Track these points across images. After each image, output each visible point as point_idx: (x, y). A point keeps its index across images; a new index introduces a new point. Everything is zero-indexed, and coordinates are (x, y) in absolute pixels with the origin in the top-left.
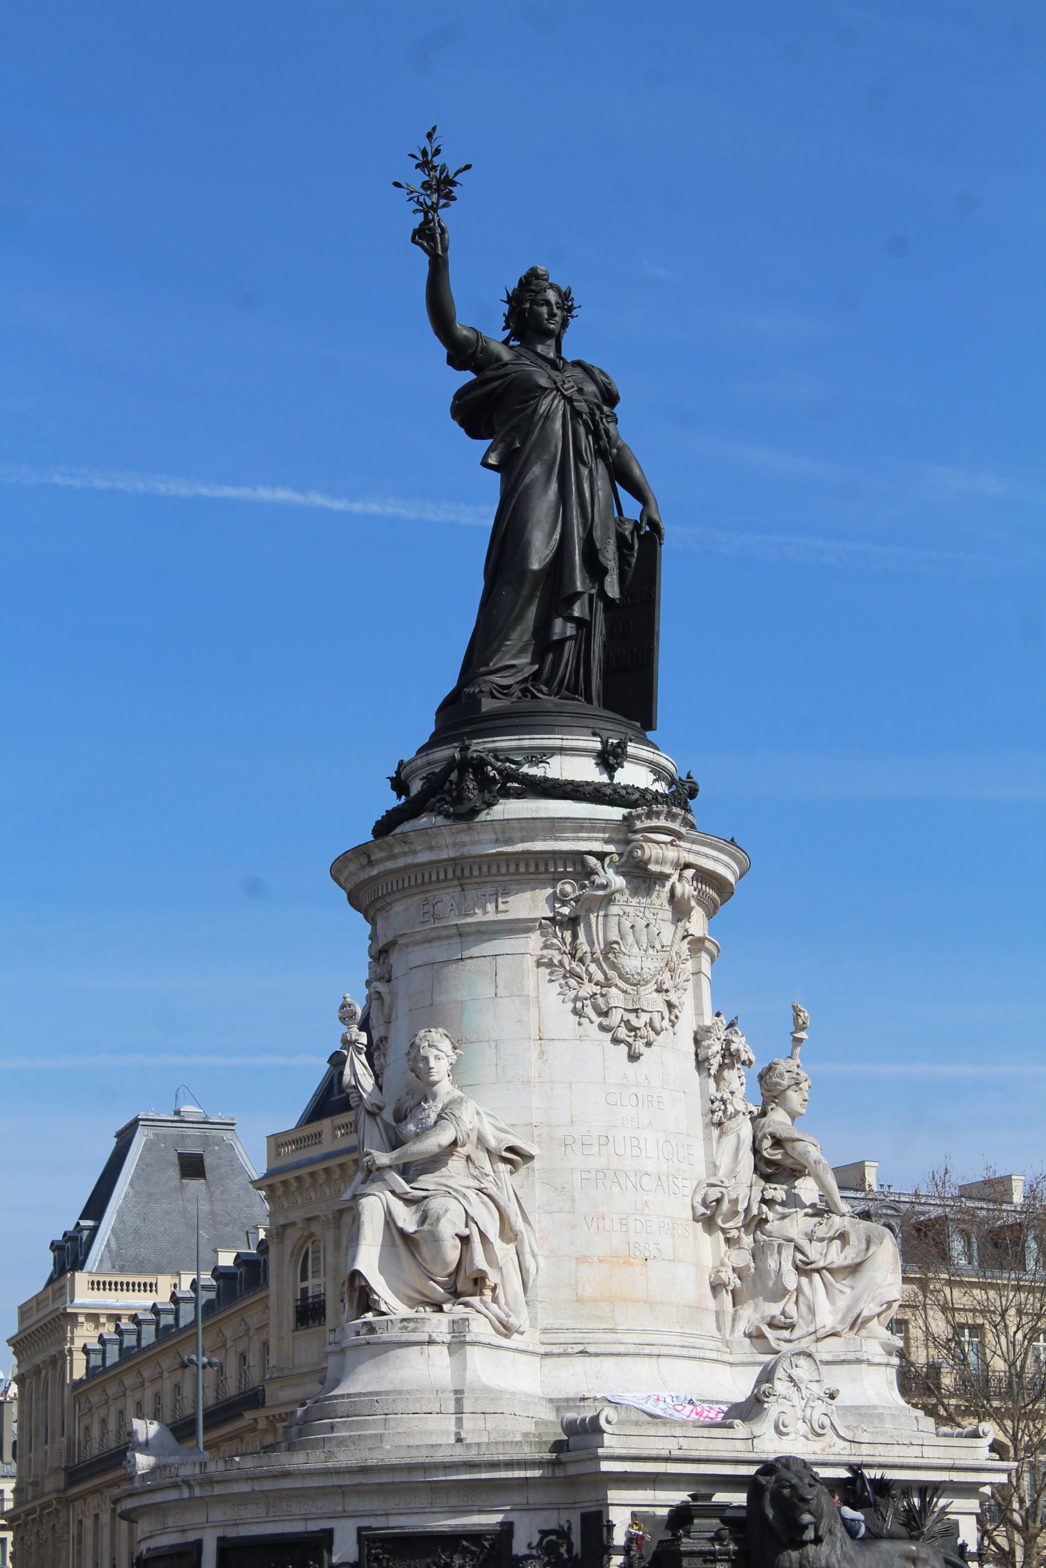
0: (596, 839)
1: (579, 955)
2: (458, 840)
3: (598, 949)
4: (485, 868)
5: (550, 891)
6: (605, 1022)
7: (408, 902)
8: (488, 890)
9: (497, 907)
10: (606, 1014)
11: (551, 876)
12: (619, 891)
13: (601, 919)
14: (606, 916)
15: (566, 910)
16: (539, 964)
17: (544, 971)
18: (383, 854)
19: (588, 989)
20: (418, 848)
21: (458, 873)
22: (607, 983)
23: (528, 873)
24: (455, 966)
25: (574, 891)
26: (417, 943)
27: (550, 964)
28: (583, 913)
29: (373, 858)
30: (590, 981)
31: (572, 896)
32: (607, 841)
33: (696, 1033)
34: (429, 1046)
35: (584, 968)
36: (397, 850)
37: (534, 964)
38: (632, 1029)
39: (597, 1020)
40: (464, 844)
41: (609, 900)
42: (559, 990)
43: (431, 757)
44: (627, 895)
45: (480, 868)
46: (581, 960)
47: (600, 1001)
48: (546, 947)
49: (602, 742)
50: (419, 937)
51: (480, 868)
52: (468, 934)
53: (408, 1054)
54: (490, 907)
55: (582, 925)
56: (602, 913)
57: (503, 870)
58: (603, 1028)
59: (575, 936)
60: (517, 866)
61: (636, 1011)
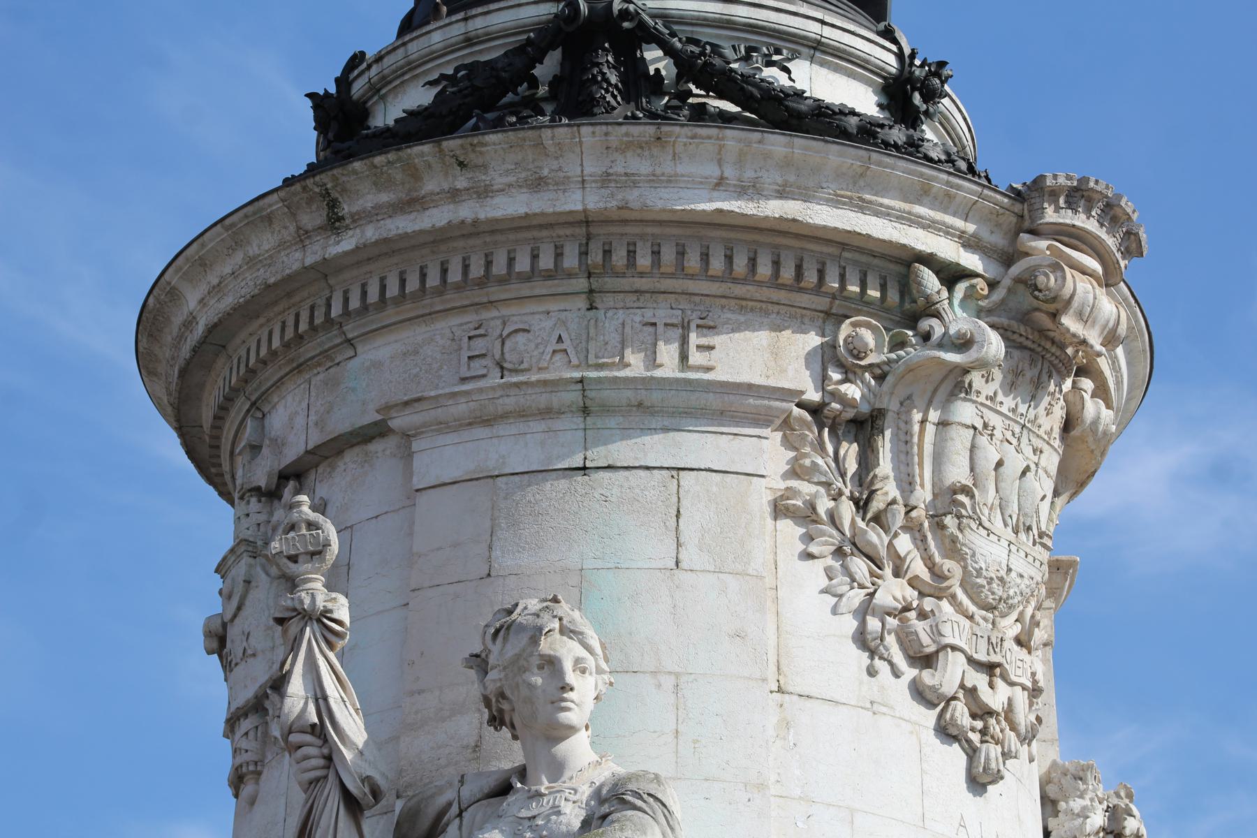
0: (947, 231)
1: (877, 504)
2: (619, 168)
3: (923, 495)
4: (668, 255)
5: (813, 340)
6: (928, 677)
7: (418, 333)
8: (662, 314)
9: (684, 357)
10: (926, 661)
11: (822, 303)
12: (982, 364)
13: (930, 429)
14: (943, 424)
15: (853, 391)
16: (780, 509)
17: (790, 531)
18: (384, 197)
19: (893, 591)
20: (500, 182)
21: (596, 257)
22: (936, 586)
23: (775, 281)
24: (563, 484)
25: (879, 348)
26: (444, 427)
27: (807, 516)
28: (894, 406)
29: (346, 209)
30: (897, 574)
31: (872, 359)
32: (970, 243)
33: (1045, 783)
34: (563, 631)
35: (886, 540)
36: (431, 185)
37: (768, 510)
38: (982, 712)
39: (910, 673)
40: (631, 180)
41: (955, 384)
42: (824, 582)
43: (478, 24)
44: (994, 386)
45: (656, 253)
46: (877, 519)
47: (921, 627)
48: (795, 472)
49: (900, 55)
50: (461, 408)
51: (656, 253)
52: (607, 409)
53: (479, 662)
54: (668, 353)
55: (888, 433)
56: (934, 416)
57: (717, 264)
58: (920, 693)
59: (867, 461)
60: (753, 262)
61: (990, 668)
